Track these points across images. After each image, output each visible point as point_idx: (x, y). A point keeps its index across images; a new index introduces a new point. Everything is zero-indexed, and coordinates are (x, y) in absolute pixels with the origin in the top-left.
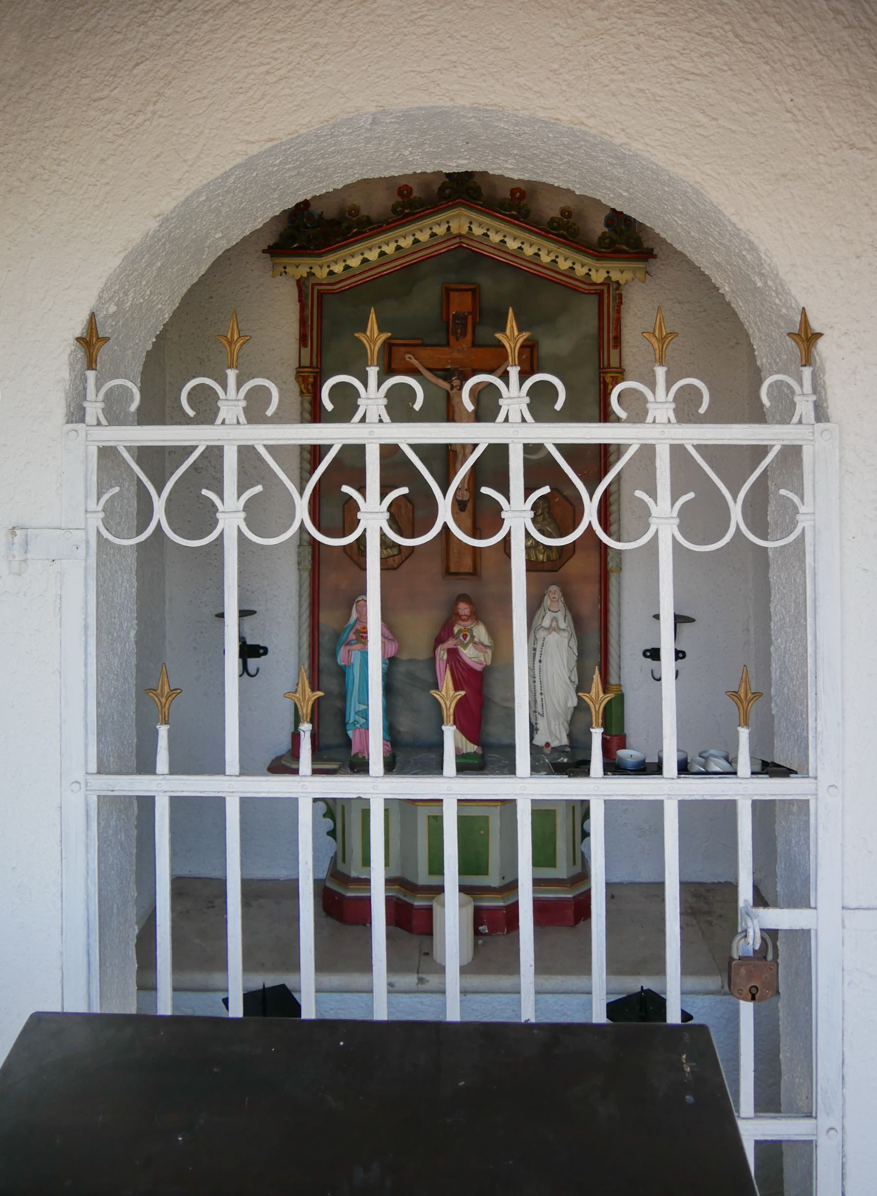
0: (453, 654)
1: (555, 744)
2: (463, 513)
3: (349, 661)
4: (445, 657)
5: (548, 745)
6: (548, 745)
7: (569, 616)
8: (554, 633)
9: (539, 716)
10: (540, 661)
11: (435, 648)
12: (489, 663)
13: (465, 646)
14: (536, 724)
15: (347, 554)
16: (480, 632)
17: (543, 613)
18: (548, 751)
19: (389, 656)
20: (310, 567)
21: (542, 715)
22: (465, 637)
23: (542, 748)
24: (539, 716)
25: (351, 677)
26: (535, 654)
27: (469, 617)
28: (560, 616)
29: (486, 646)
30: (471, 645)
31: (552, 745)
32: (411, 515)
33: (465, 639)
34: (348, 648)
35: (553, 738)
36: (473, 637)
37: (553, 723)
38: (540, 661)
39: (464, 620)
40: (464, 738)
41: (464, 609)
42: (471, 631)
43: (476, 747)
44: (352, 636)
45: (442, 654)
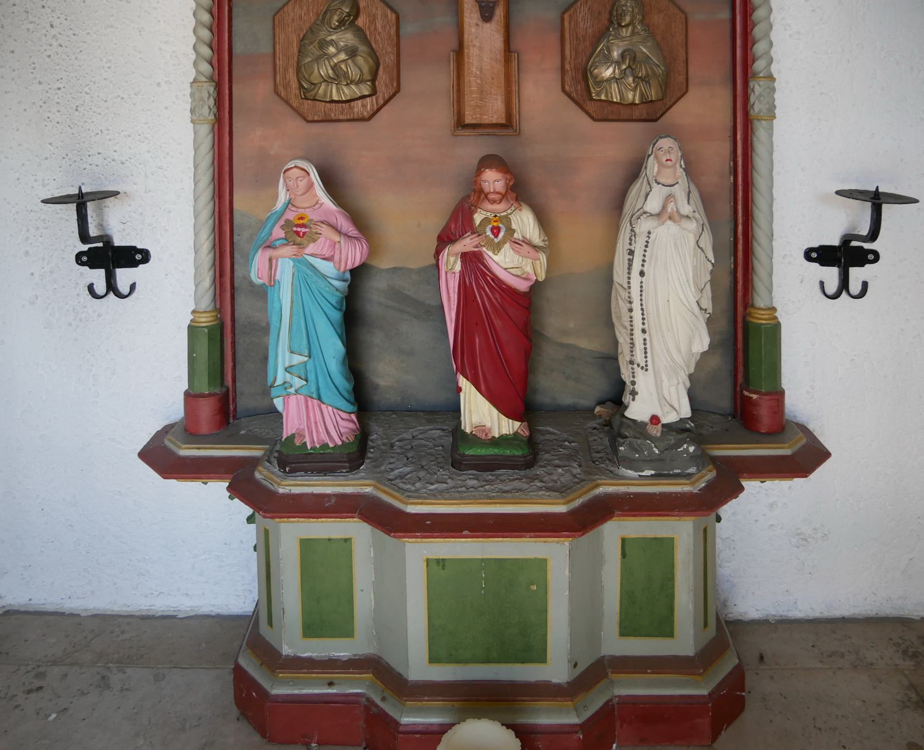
0: (472, 260)
1: (669, 418)
2: (488, 25)
3: (272, 277)
4: (458, 267)
5: (655, 419)
6: (655, 419)
7: (695, 194)
8: (669, 222)
9: (638, 370)
10: (642, 274)
11: (438, 252)
12: (542, 277)
13: (497, 248)
14: (633, 383)
15: (279, 95)
16: (525, 222)
17: (645, 188)
18: (656, 431)
19: (349, 266)
20: (212, 117)
21: (645, 368)
22: (496, 231)
23: (643, 425)
24: (638, 370)
25: (276, 305)
26: (630, 261)
27: (504, 197)
28: (680, 191)
29: (535, 247)
30: (507, 246)
31: (665, 420)
32: (393, 31)
33: (496, 236)
34: (269, 253)
35: (668, 408)
36: (510, 231)
37: (666, 383)
38: (642, 274)
39: (493, 202)
40: (495, 411)
41: (493, 180)
42: (507, 220)
43: (517, 424)
44: (279, 233)
45: (451, 263)
